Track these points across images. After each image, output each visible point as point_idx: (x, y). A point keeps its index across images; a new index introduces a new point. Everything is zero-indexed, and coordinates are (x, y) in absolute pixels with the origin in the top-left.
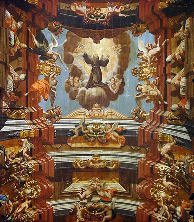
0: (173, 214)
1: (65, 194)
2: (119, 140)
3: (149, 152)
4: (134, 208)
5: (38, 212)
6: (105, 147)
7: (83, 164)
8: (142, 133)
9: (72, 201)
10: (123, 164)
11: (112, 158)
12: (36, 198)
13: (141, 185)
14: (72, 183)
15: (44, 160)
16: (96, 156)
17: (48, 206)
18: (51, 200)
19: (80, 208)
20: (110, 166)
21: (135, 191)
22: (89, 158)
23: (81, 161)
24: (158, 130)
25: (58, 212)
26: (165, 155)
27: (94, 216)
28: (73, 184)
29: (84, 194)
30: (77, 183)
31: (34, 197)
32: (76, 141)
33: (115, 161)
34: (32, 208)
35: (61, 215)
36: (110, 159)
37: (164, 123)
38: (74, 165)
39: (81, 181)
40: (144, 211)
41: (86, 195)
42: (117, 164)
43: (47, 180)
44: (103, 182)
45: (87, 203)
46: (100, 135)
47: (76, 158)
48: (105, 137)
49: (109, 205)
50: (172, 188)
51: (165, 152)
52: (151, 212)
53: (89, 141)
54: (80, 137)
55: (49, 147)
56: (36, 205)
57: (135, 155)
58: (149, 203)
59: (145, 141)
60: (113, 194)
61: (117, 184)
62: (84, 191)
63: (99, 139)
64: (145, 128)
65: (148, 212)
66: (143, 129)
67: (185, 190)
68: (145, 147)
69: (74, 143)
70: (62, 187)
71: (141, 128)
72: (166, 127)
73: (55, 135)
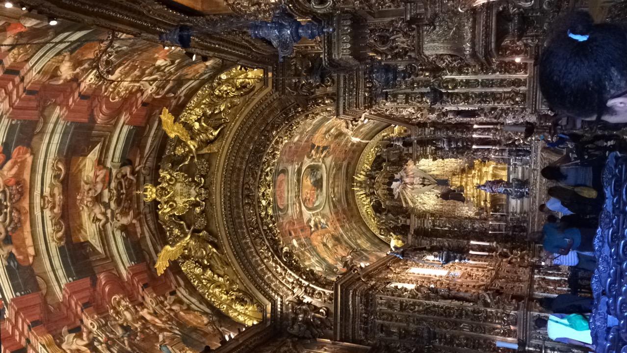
0: (158, 71)
1: (105, 251)
2: (19, 158)
3: (55, 101)
4: (126, 129)
5: (143, 290)
6: (29, 187)
7: (58, 227)
8: (19, 111)
9: (111, 235)
10: (60, 151)
11: (49, 172)
12: (129, 299)
13: (98, 116)
14: (88, 241)
15: (73, 303)
16: (44, 204)
17: (130, 276)
18: (120, 276)
19: (118, 221)
20: (59, 176)
21: (104, 127)
22: (48, 216)
23: (54, 230)
24: (27, 80)
25: (131, 259)
26: (75, 72)
27: (127, 196)
28: (89, 240)
29: (100, 216)
30: (86, 232)
31: (130, 303)
32: (21, 247)
33: (53, 166)
34: (144, 303)
35: (132, 251)
36: (49, 174)
37: (23, 68)
38: (62, 243)
39: (82, 225)
40: (134, 113)
41: (100, 213)
42: (60, 160)
43: (98, 288)
44: (84, 186)
45: (112, 210)
46: (8, 198)
47: (51, 241)
48: (11, 188)
49: (114, 172)
50: (128, 68)
51: (72, 72)
52: (140, 102)
53: (20, 221)
54: (14, 241)
55: (49, 300)
56: (136, 296)
57: (50, 126)
58: (127, 105)
59: (35, 106)
60: (101, 166)
61: (88, 160)
62: (97, 218)
63: (14, 201)
64: (11, 105)
65: (136, 108)
66: (11, 109)
67: (145, 51)
68: (44, 108)
69: (26, 251)
70: (98, 258)
71: (8, 114)
72: (31, 65)
73: (25, 294)
